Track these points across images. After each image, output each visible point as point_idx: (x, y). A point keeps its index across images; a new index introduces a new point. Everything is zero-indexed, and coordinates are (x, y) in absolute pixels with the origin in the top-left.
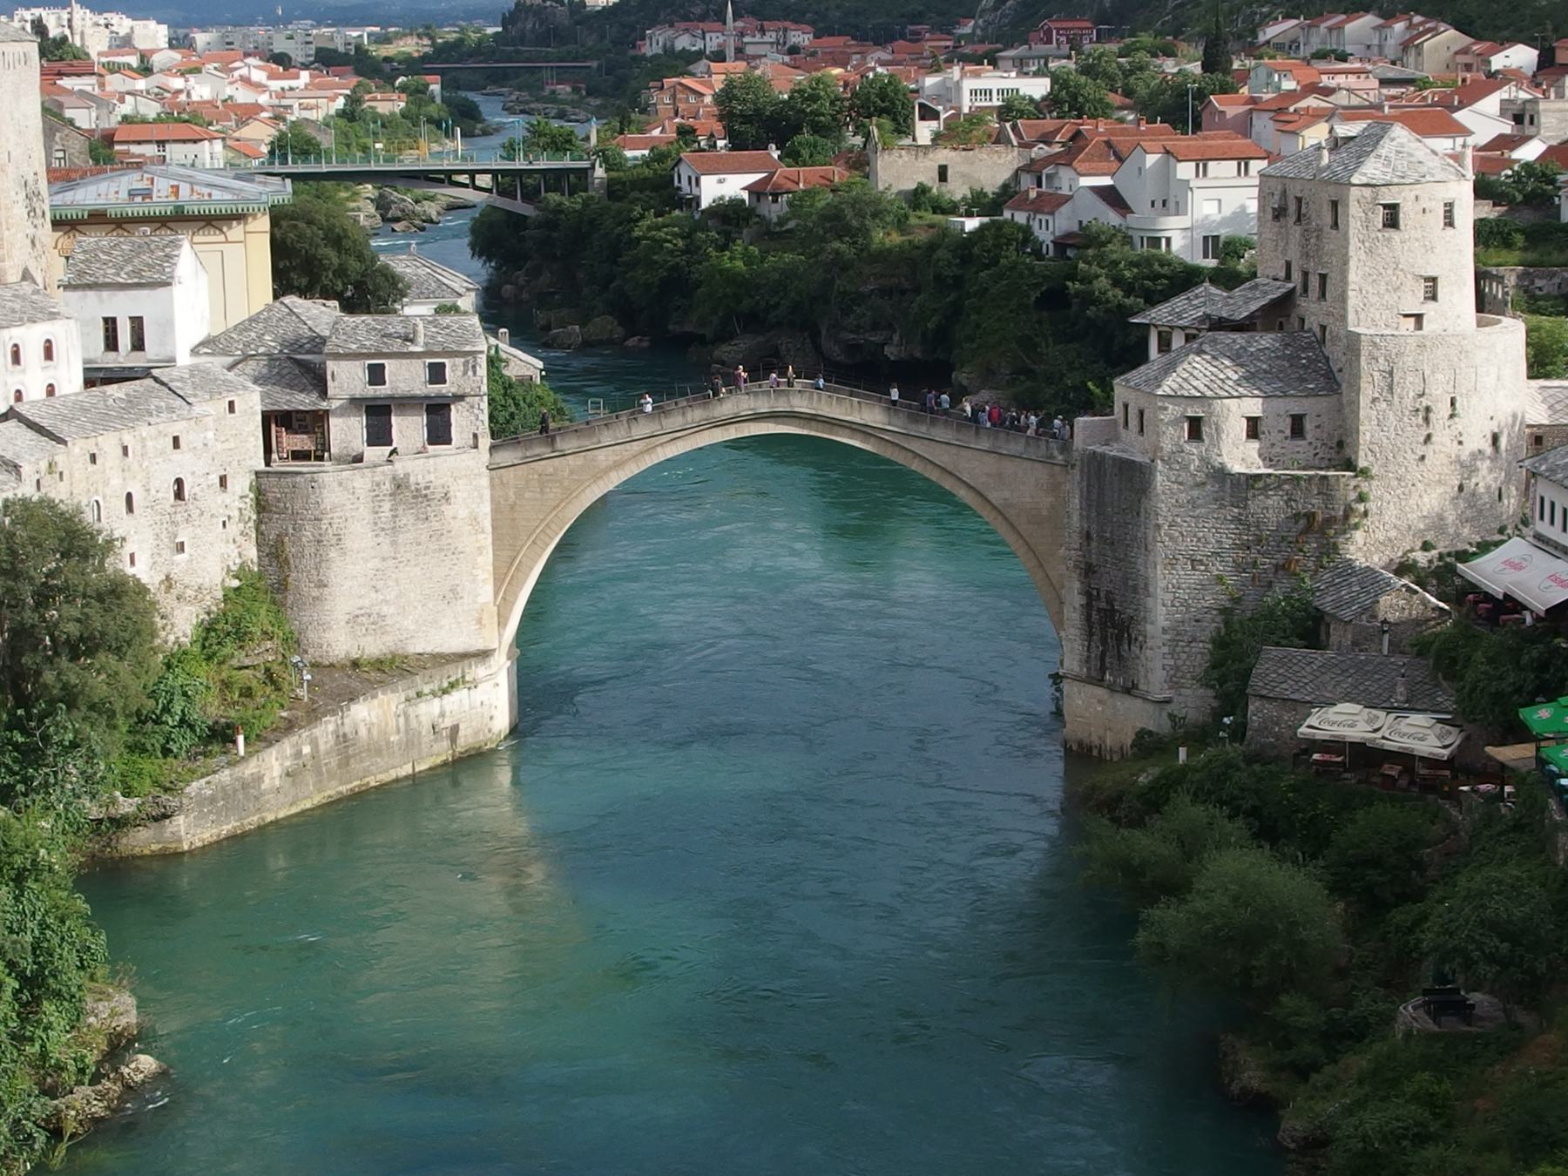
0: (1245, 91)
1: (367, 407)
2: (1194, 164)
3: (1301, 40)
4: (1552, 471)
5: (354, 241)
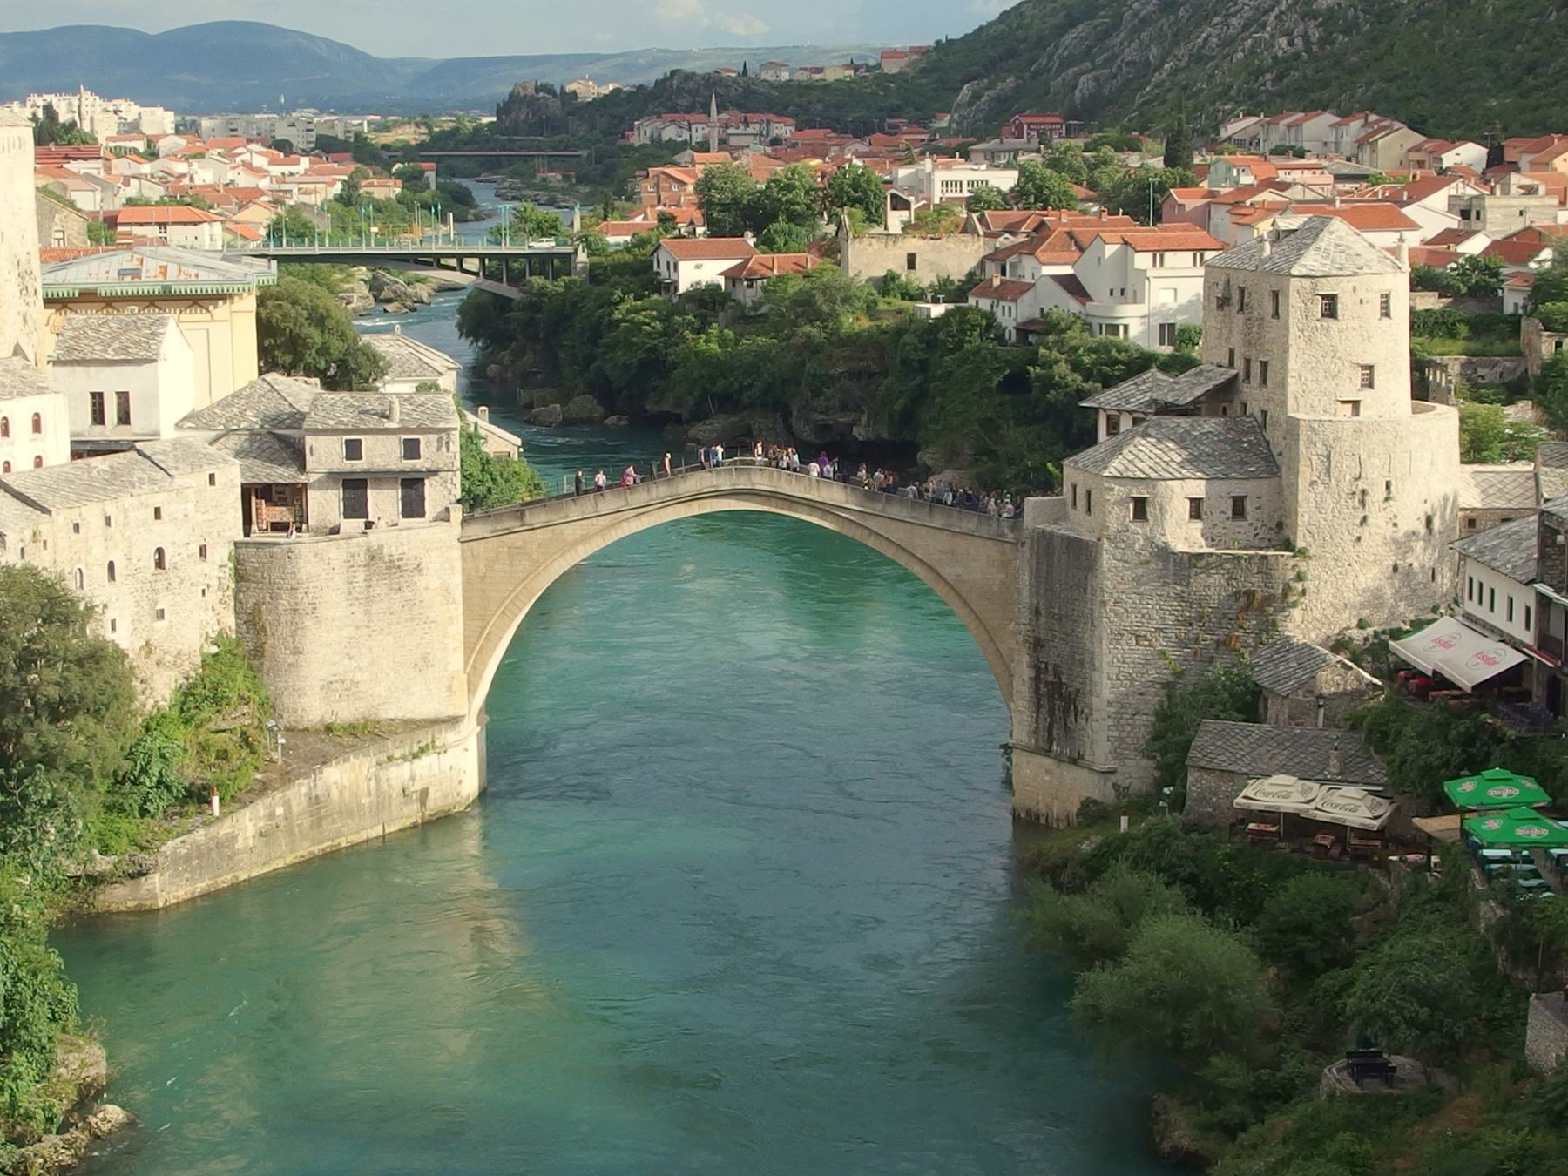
0: (1205, 185)
1: (345, 482)
2: (1151, 254)
3: (1262, 137)
4: (1481, 552)
5: (337, 322)
